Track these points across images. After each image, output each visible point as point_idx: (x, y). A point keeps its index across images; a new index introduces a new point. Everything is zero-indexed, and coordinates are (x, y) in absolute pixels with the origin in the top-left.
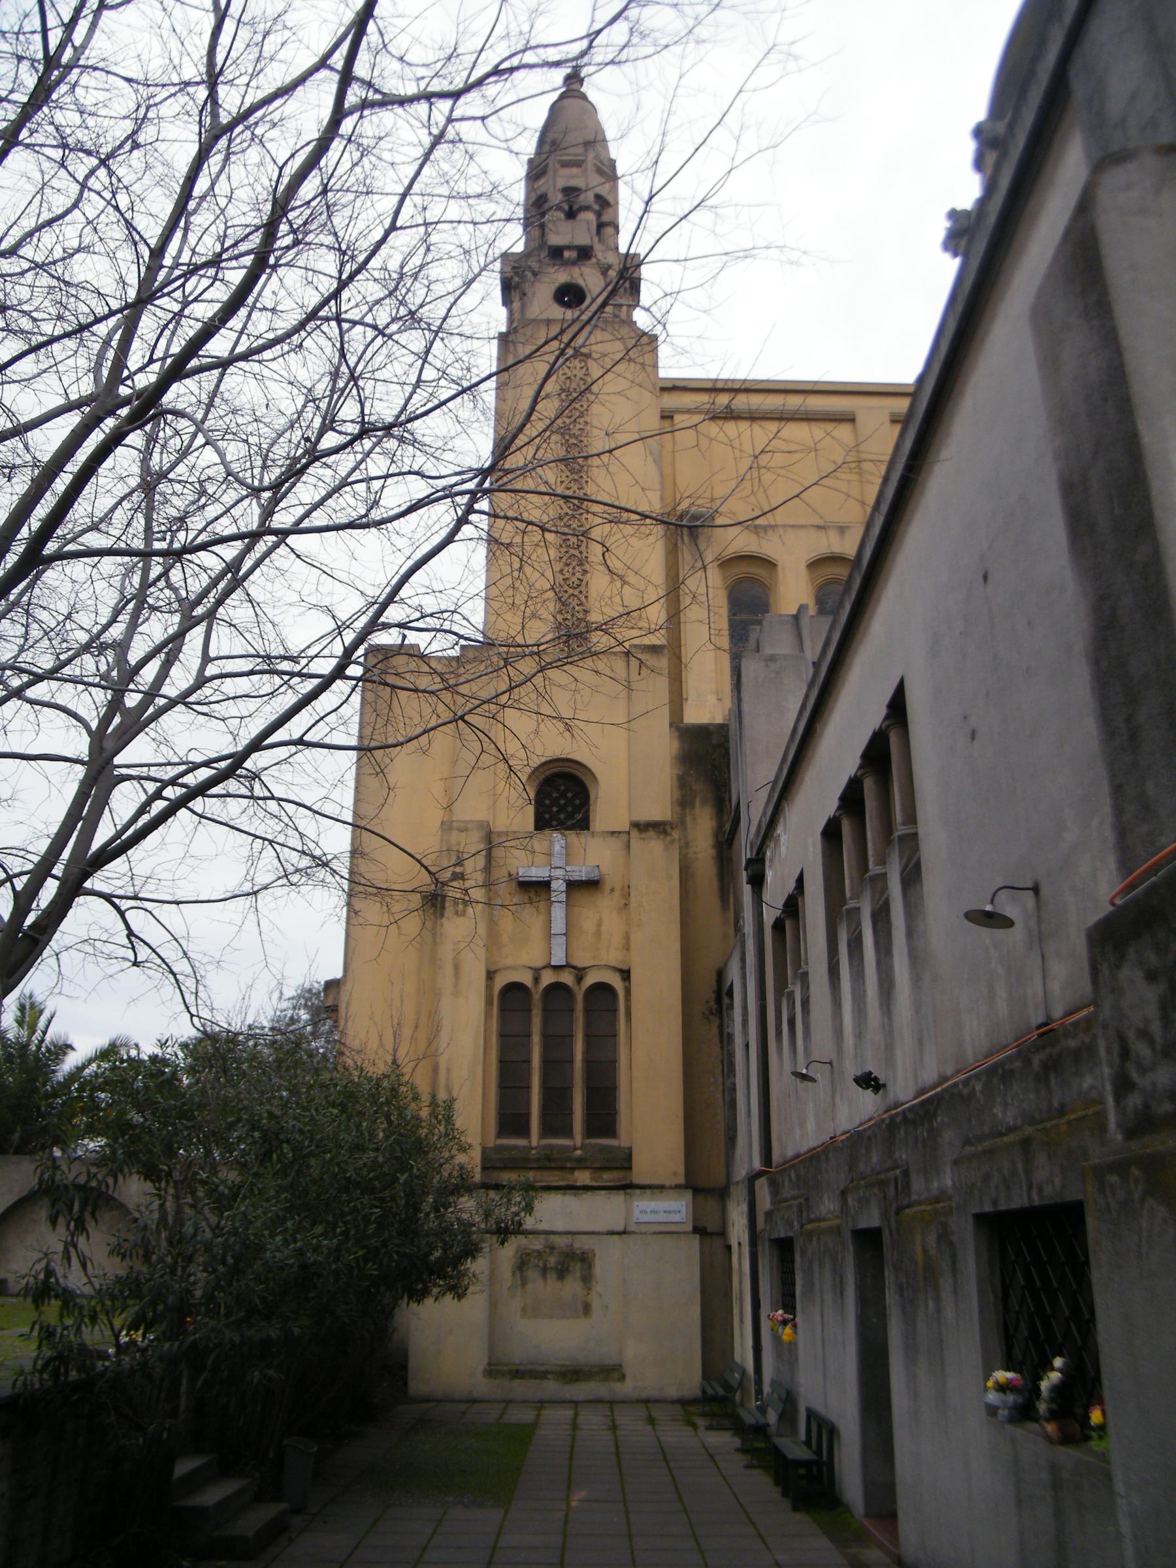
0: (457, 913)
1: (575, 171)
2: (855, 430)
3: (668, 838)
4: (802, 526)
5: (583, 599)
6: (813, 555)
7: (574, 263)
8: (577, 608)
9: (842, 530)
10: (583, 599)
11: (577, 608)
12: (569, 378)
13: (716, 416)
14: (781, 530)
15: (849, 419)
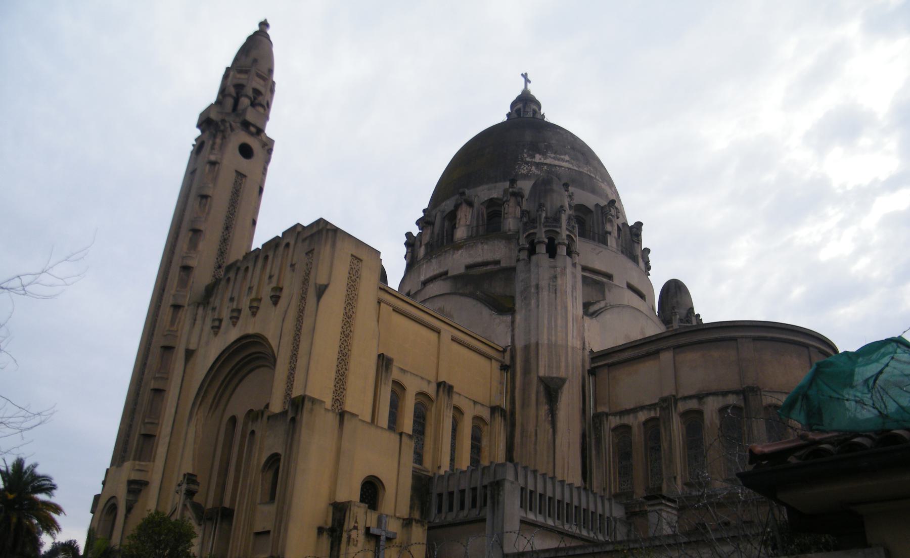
0: (354, 545)
1: (262, 82)
2: (439, 337)
3: (424, 528)
4: (417, 375)
5: (344, 383)
6: (418, 390)
7: (252, 134)
8: (341, 386)
9: (429, 382)
10: (344, 383)
11: (341, 386)
12: (352, 268)
13: (396, 310)
14: (409, 374)
15: (438, 332)
